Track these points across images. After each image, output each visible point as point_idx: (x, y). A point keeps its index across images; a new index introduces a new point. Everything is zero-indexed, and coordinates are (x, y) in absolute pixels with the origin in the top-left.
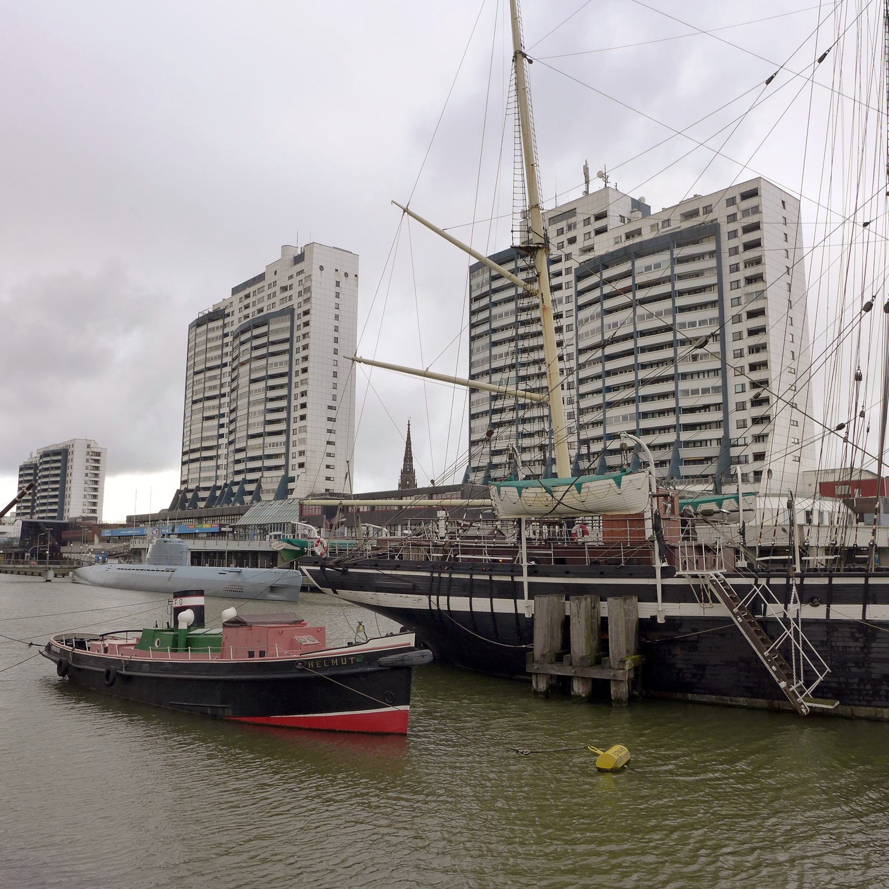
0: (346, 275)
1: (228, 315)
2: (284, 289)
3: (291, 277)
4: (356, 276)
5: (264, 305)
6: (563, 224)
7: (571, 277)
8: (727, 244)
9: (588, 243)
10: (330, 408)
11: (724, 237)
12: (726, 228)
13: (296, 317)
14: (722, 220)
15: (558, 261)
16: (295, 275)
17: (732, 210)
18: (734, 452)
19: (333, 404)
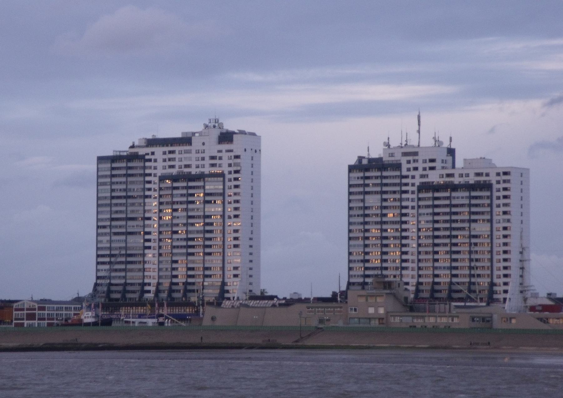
0: (256, 151)
1: (150, 160)
2: (213, 158)
3: (220, 151)
4: (260, 150)
5: (194, 163)
6: (411, 158)
7: (415, 189)
8: (495, 194)
9: (424, 173)
10: (251, 239)
11: (494, 190)
12: (495, 186)
13: (227, 180)
14: (494, 182)
15: (407, 177)
16: (224, 151)
17: (498, 178)
18: (495, 288)
19: (251, 236)
